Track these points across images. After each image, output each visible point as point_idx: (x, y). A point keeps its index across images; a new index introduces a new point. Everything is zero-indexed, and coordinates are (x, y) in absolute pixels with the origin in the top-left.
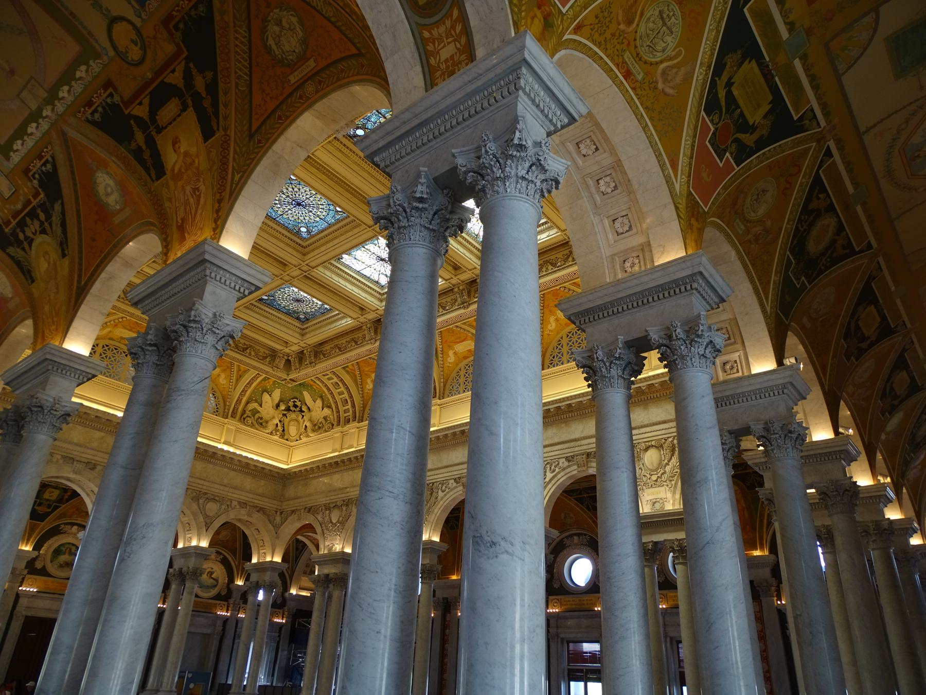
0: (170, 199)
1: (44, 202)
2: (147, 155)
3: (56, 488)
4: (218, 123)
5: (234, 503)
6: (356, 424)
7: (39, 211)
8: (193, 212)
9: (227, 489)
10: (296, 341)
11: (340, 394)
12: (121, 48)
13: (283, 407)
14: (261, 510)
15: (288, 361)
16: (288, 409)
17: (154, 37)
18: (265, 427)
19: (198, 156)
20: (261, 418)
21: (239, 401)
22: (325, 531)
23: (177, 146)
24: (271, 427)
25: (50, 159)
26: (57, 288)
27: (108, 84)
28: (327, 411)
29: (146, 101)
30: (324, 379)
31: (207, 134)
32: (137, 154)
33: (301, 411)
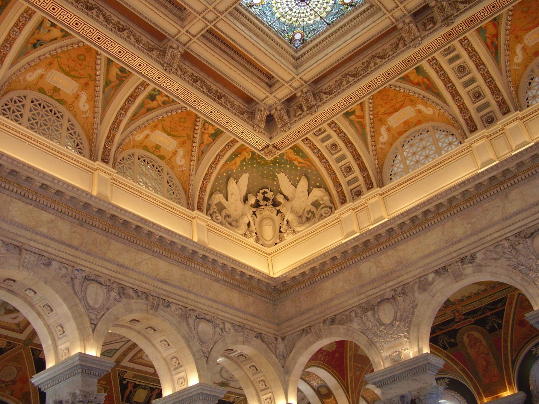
6: (377, 190)
9: (215, 305)
10: (288, 78)
11: (338, 160)
13: (252, 200)
14: (259, 336)
15: (270, 119)
16: (257, 205)
18: (237, 227)
20: (229, 216)
21: (203, 189)
22: (376, 339)
24: (244, 227)
28: (317, 193)
30: (316, 141)
33: (275, 204)
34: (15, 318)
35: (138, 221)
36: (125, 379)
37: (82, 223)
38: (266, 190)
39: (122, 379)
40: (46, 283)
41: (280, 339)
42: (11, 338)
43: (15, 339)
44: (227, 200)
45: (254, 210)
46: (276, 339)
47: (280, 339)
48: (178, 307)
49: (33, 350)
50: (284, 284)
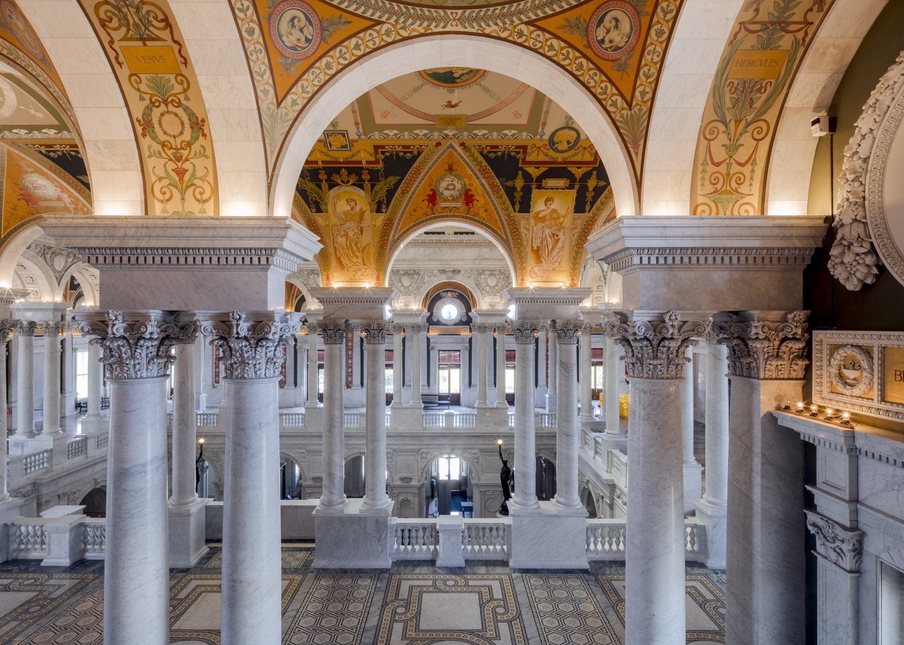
0: (528, 229)
1: (378, 171)
2: (518, 195)
4: (591, 209)
7: (365, 172)
8: (550, 247)
12: (555, 139)
17: (585, 148)
19: (564, 217)
23: (549, 203)
25: (416, 152)
26: (362, 231)
27: (525, 148)
29: (543, 169)
31: (579, 208)
32: (510, 191)
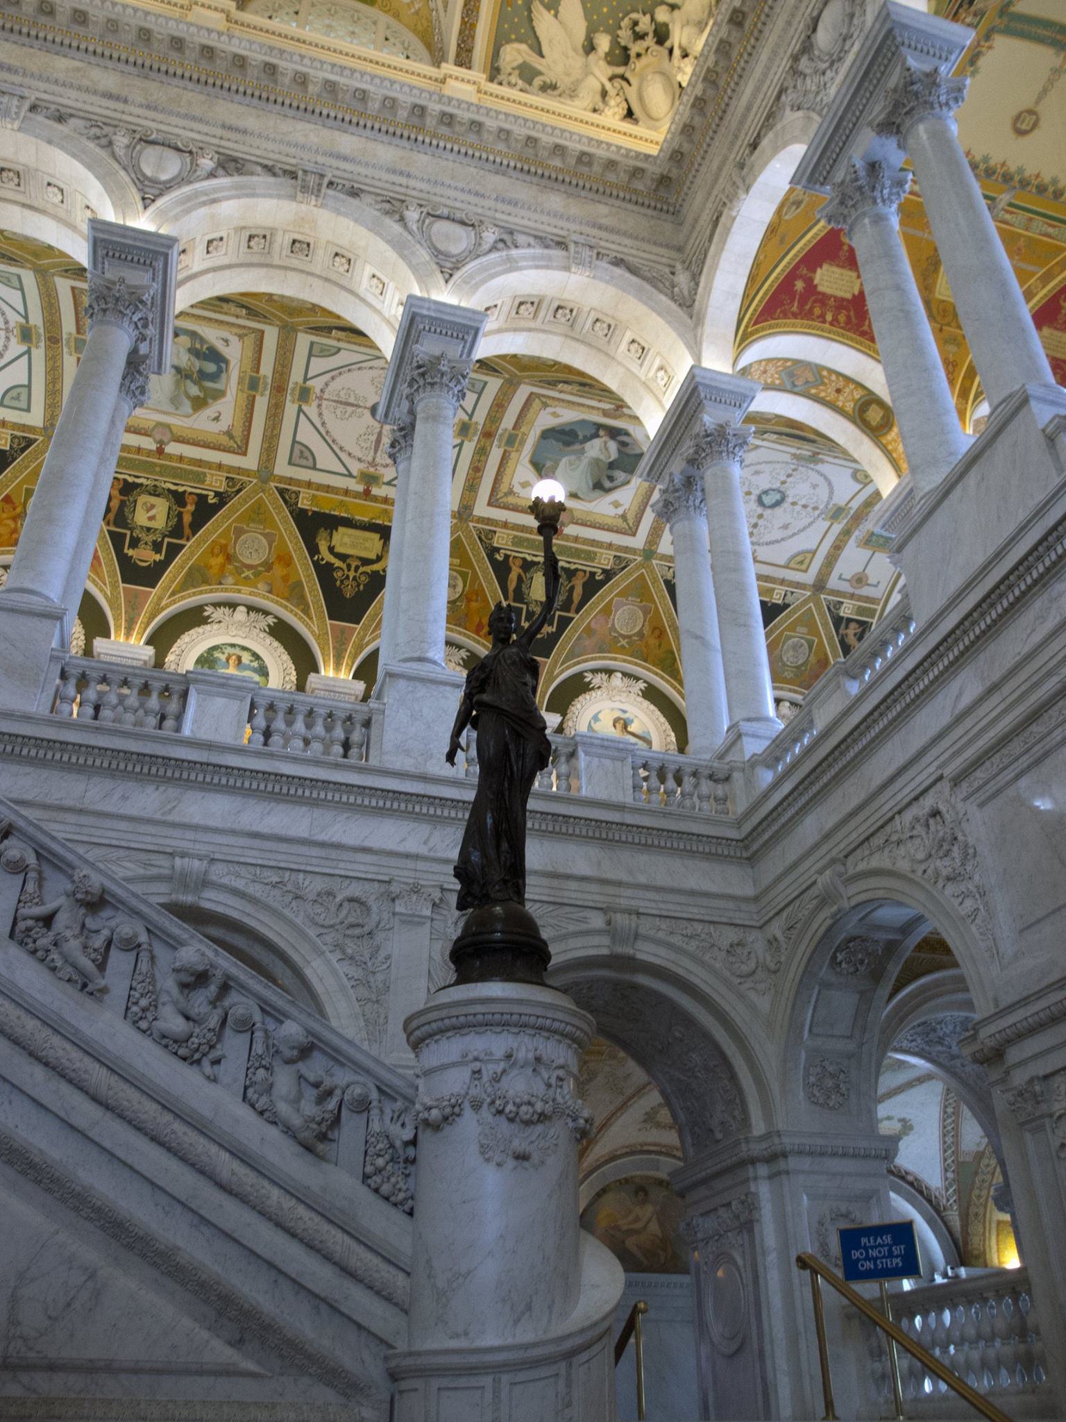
3: (155, 492)
5: (521, 239)
13: (603, 43)
20: (554, 87)
34: (217, 419)
35: (265, 54)
36: (498, 550)
37: (146, 70)
38: (634, 16)
39: (492, 551)
40: (50, 142)
41: (679, 266)
42: (231, 469)
43: (239, 470)
44: (543, 56)
45: (620, 70)
46: (673, 273)
47: (679, 266)
48: (379, 198)
49: (282, 492)
50: (677, 156)
